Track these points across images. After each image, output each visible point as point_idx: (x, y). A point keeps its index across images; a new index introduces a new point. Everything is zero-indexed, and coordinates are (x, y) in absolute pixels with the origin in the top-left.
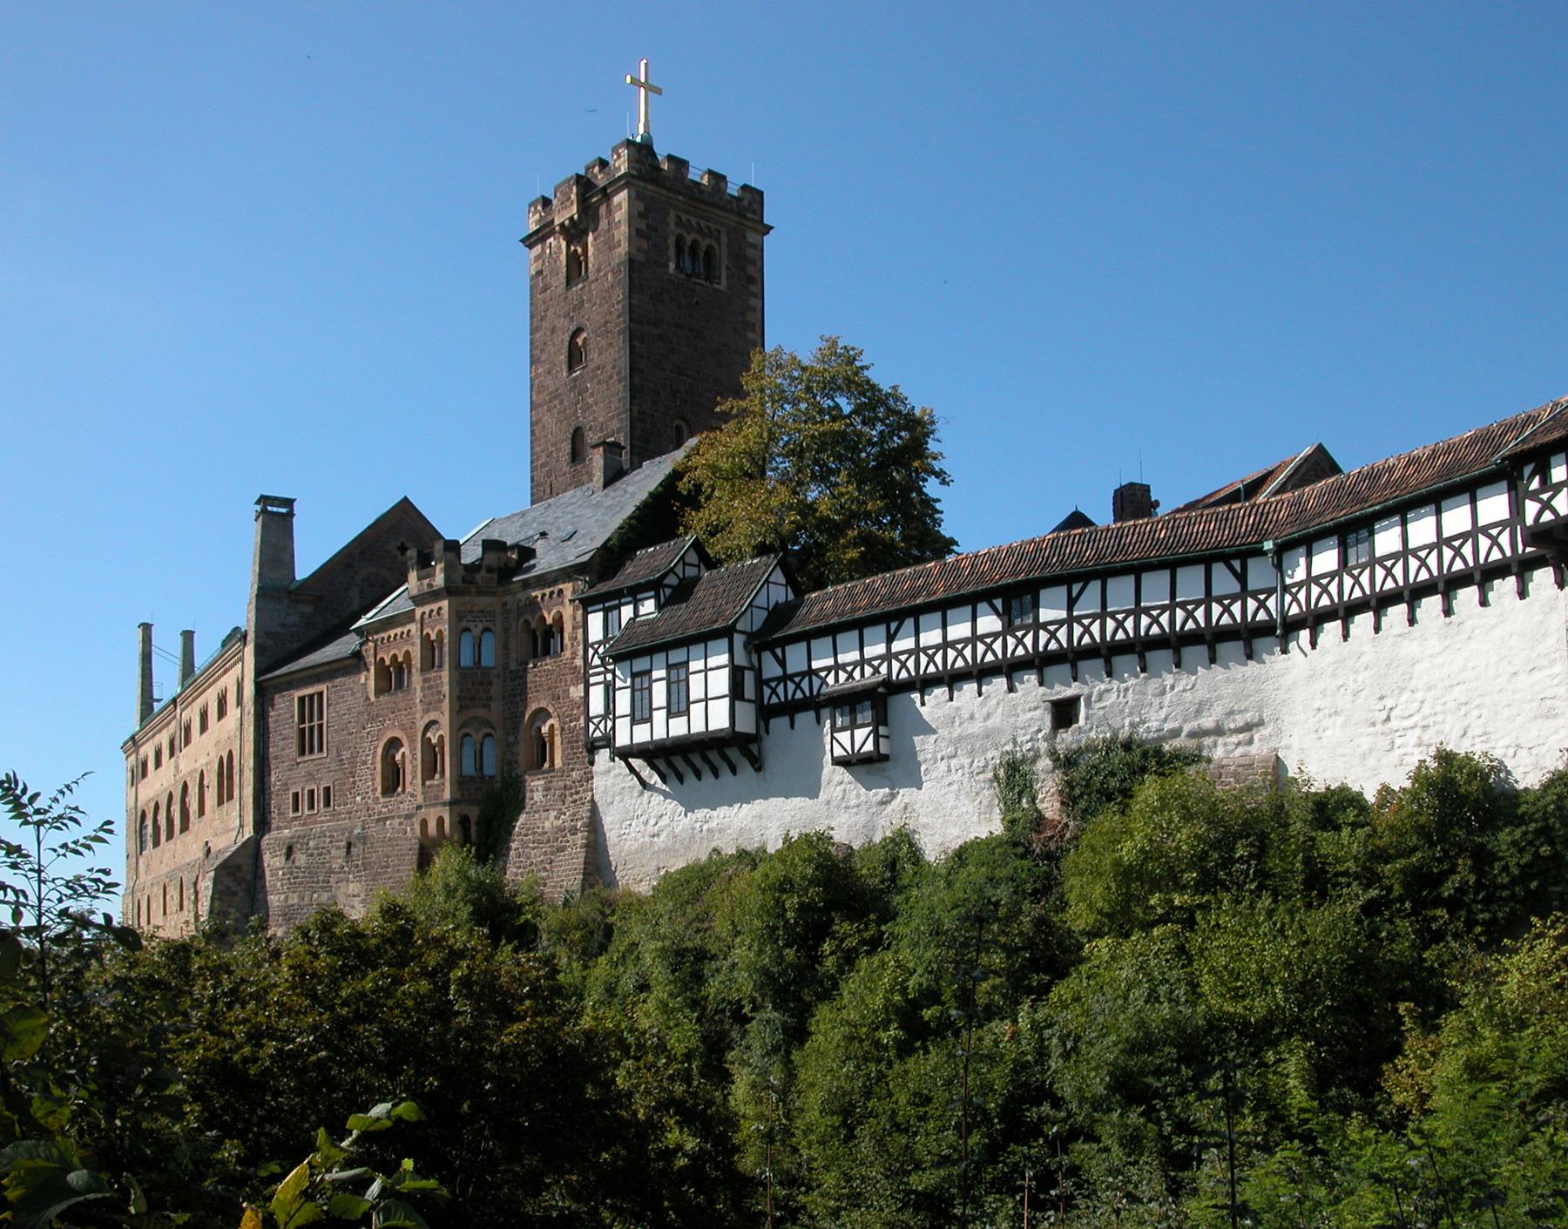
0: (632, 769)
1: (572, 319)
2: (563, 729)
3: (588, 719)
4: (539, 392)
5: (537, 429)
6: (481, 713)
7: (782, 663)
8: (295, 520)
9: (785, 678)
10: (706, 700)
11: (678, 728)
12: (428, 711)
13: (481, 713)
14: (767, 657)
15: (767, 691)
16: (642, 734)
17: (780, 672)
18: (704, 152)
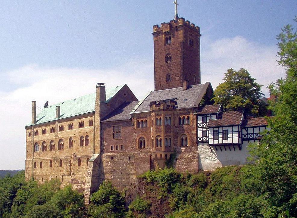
0: (211, 148)
1: (166, 52)
2: (190, 139)
3: (197, 137)
4: (157, 65)
5: (156, 72)
6: (169, 134)
7: (247, 131)
8: (106, 88)
9: (248, 134)
10: (232, 137)
11: (225, 142)
12: (157, 133)
13: (169, 134)
14: (244, 130)
15: (243, 136)
16: (216, 142)
17: (247, 133)
18: (194, 21)
